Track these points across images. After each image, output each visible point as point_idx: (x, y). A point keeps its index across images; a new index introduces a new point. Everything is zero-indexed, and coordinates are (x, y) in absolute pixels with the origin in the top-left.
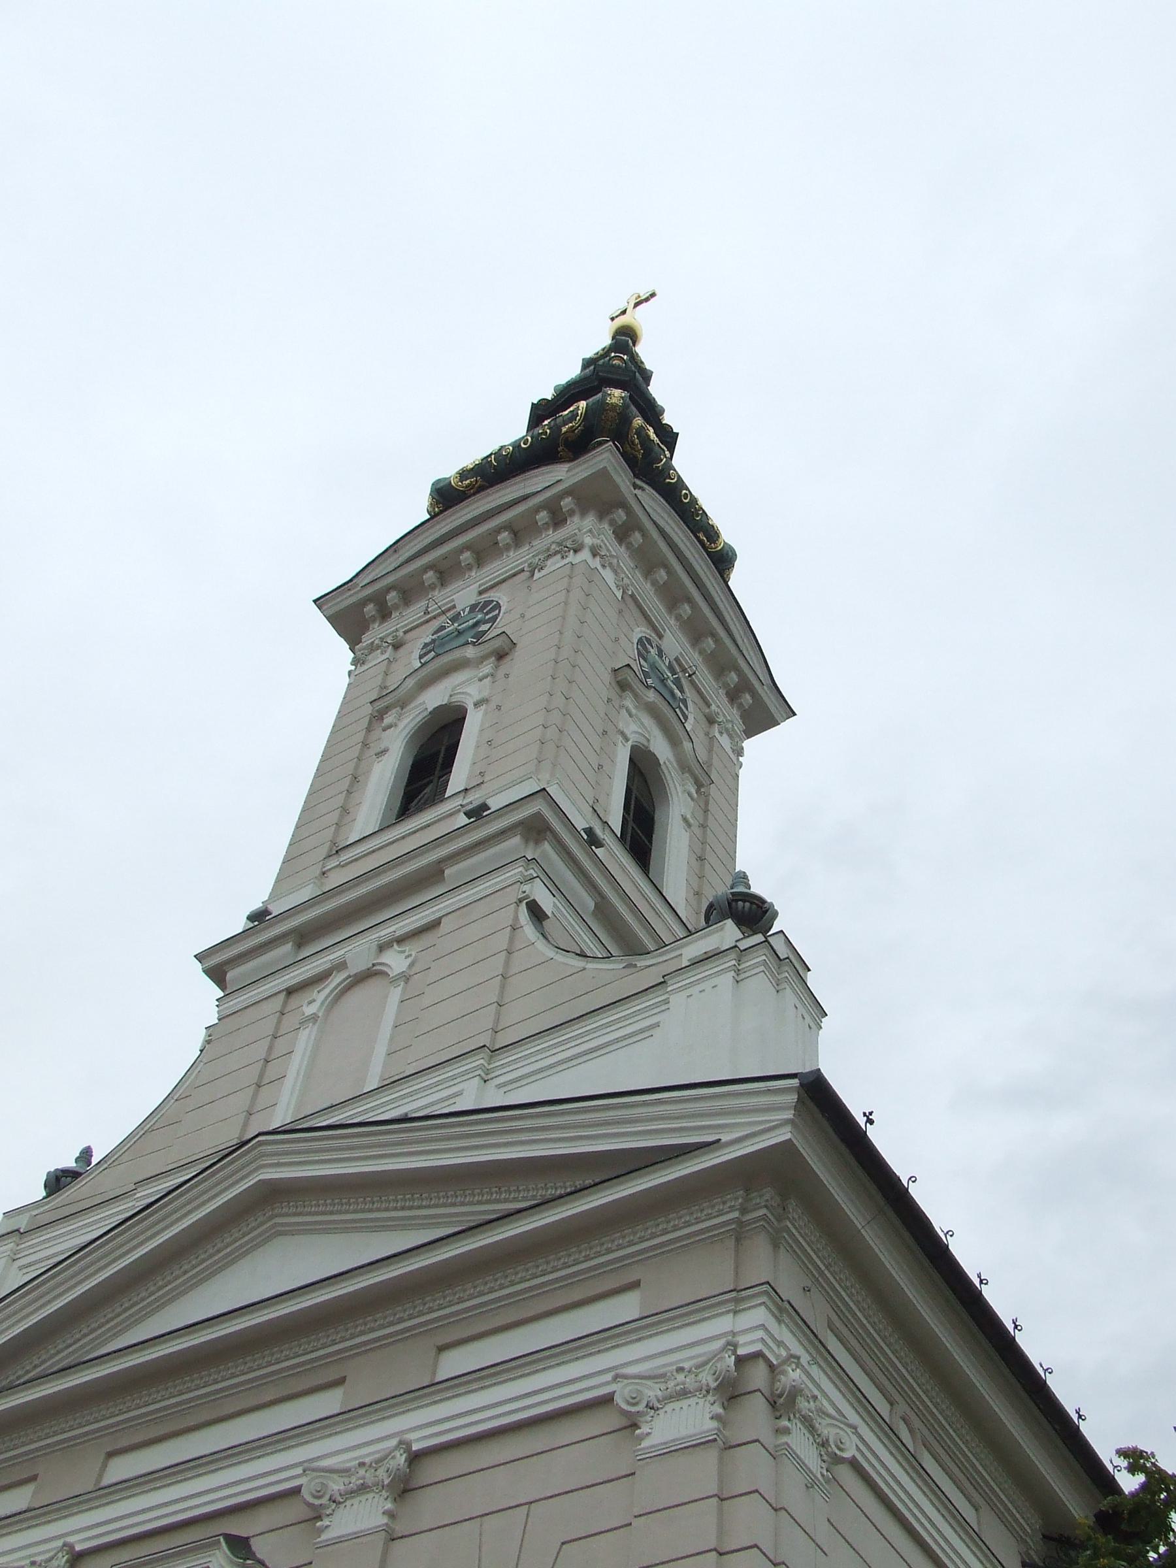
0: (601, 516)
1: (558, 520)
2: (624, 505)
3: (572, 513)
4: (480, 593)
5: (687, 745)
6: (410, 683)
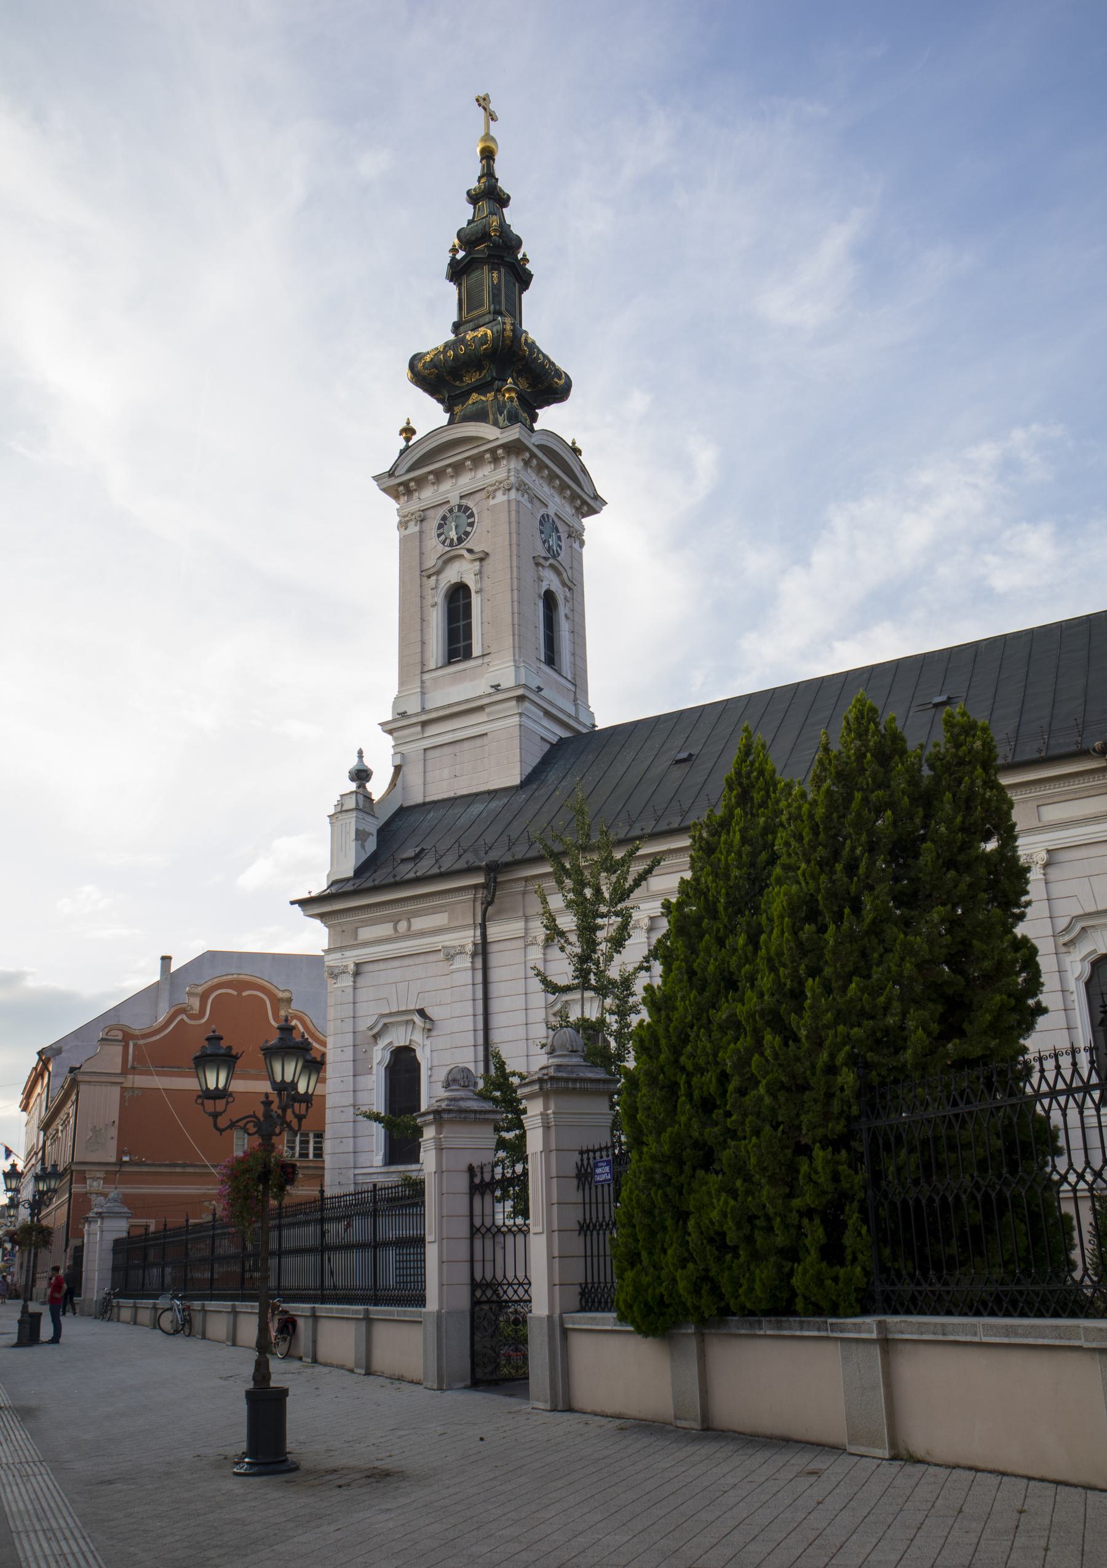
0: (517, 457)
1: (496, 460)
2: (528, 449)
3: (503, 458)
4: (461, 497)
5: (565, 575)
6: (440, 562)
